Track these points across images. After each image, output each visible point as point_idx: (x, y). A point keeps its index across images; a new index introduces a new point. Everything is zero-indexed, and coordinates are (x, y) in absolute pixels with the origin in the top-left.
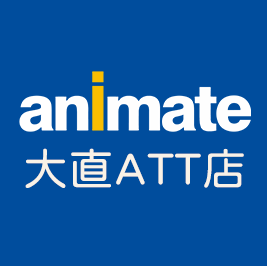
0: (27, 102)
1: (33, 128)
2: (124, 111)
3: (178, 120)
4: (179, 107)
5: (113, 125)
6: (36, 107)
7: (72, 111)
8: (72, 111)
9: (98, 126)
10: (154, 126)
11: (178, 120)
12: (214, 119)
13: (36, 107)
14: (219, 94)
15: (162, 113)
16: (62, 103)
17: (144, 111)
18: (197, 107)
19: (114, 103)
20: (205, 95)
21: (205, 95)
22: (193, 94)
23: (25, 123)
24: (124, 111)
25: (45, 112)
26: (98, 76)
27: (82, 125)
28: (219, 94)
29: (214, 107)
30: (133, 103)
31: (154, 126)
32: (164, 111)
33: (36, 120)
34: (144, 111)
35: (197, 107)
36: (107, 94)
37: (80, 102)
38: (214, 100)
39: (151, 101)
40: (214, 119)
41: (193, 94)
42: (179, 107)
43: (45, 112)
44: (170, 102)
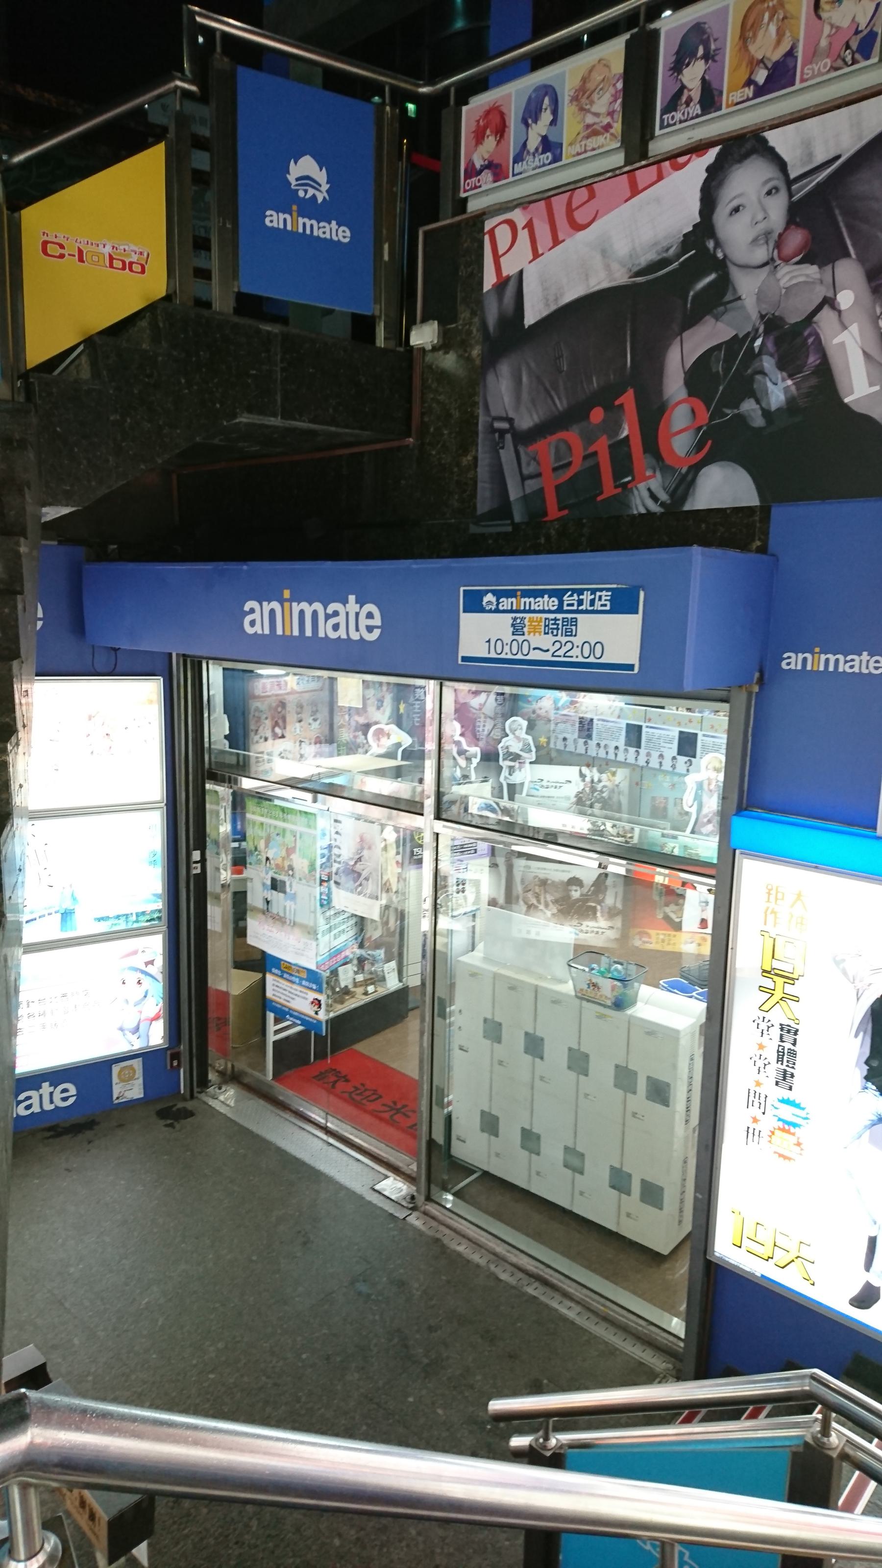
0: (785, 655)
1: (788, 668)
2: (827, 660)
3: (852, 667)
4: (853, 660)
5: (822, 668)
6: (789, 657)
7: (805, 660)
8: (805, 660)
9: (815, 669)
10: (841, 670)
11: (852, 667)
12: (867, 668)
13: (789, 657)
14: (871, 655)
15: (846, 662)
16: (801, 656)
17: (837, 661)
18: (861, 661)
19: (823, 657)
20: (865, 656)
21: (865, 656)
22: (860, 655)
23: (784, 665)
24: (827, 660)
25: (793, 660)
26: (817, 650)
27: (809, 668)
28: (871, 655)
29: (868, 661)
30: (832, 658)
31: (841, 670)
32: (846, 662)
33: (788, 664)
34: (837, 661)
35: (861, 661)
36: (820, 653)
37: (808, 656)
38: (868, 658)
39: (840, 657)
40: (867, 668)
41: (860, 655)
42: (853, 660)
43: (793, 660)
44: (849, 658)
